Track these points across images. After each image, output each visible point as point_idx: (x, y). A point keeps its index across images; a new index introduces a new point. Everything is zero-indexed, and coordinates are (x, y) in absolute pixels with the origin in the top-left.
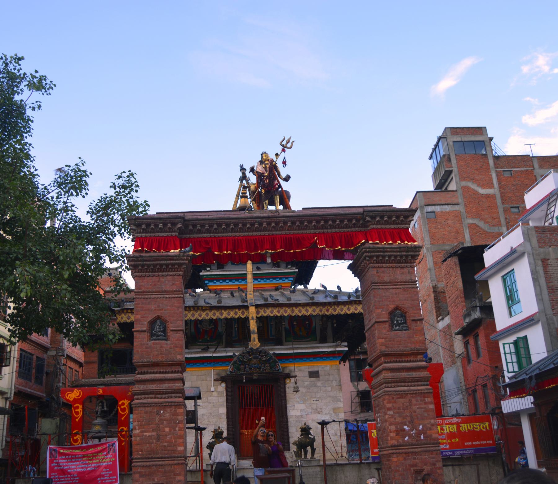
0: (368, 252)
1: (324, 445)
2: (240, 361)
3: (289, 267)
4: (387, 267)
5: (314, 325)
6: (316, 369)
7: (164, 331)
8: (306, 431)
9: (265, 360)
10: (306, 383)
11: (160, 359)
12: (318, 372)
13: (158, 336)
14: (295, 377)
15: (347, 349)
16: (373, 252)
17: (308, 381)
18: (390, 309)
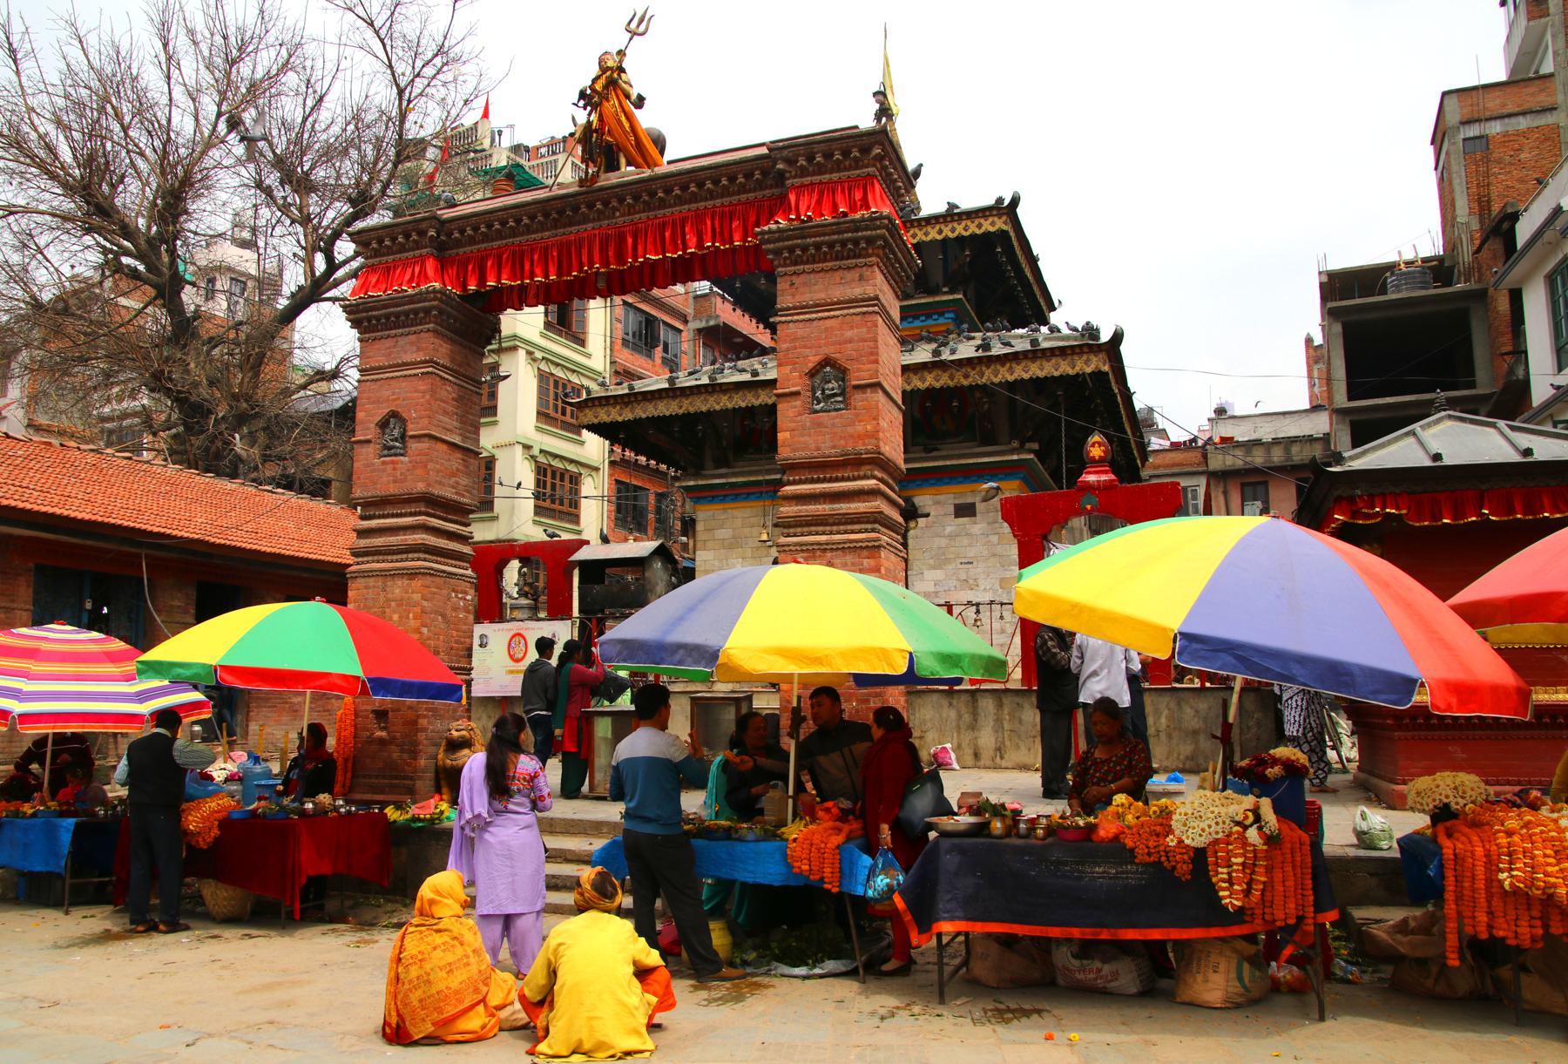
0: (768, 241)
4: (813, 271)
6: (969, 500)
7: (403, 437)
10: (949, 529)
11: (393, 490)
12: (973, 505)
13: (390, 448)
14: (927, 515)
16: (779, 240)
17: (953, 525)
18: (811, 365)
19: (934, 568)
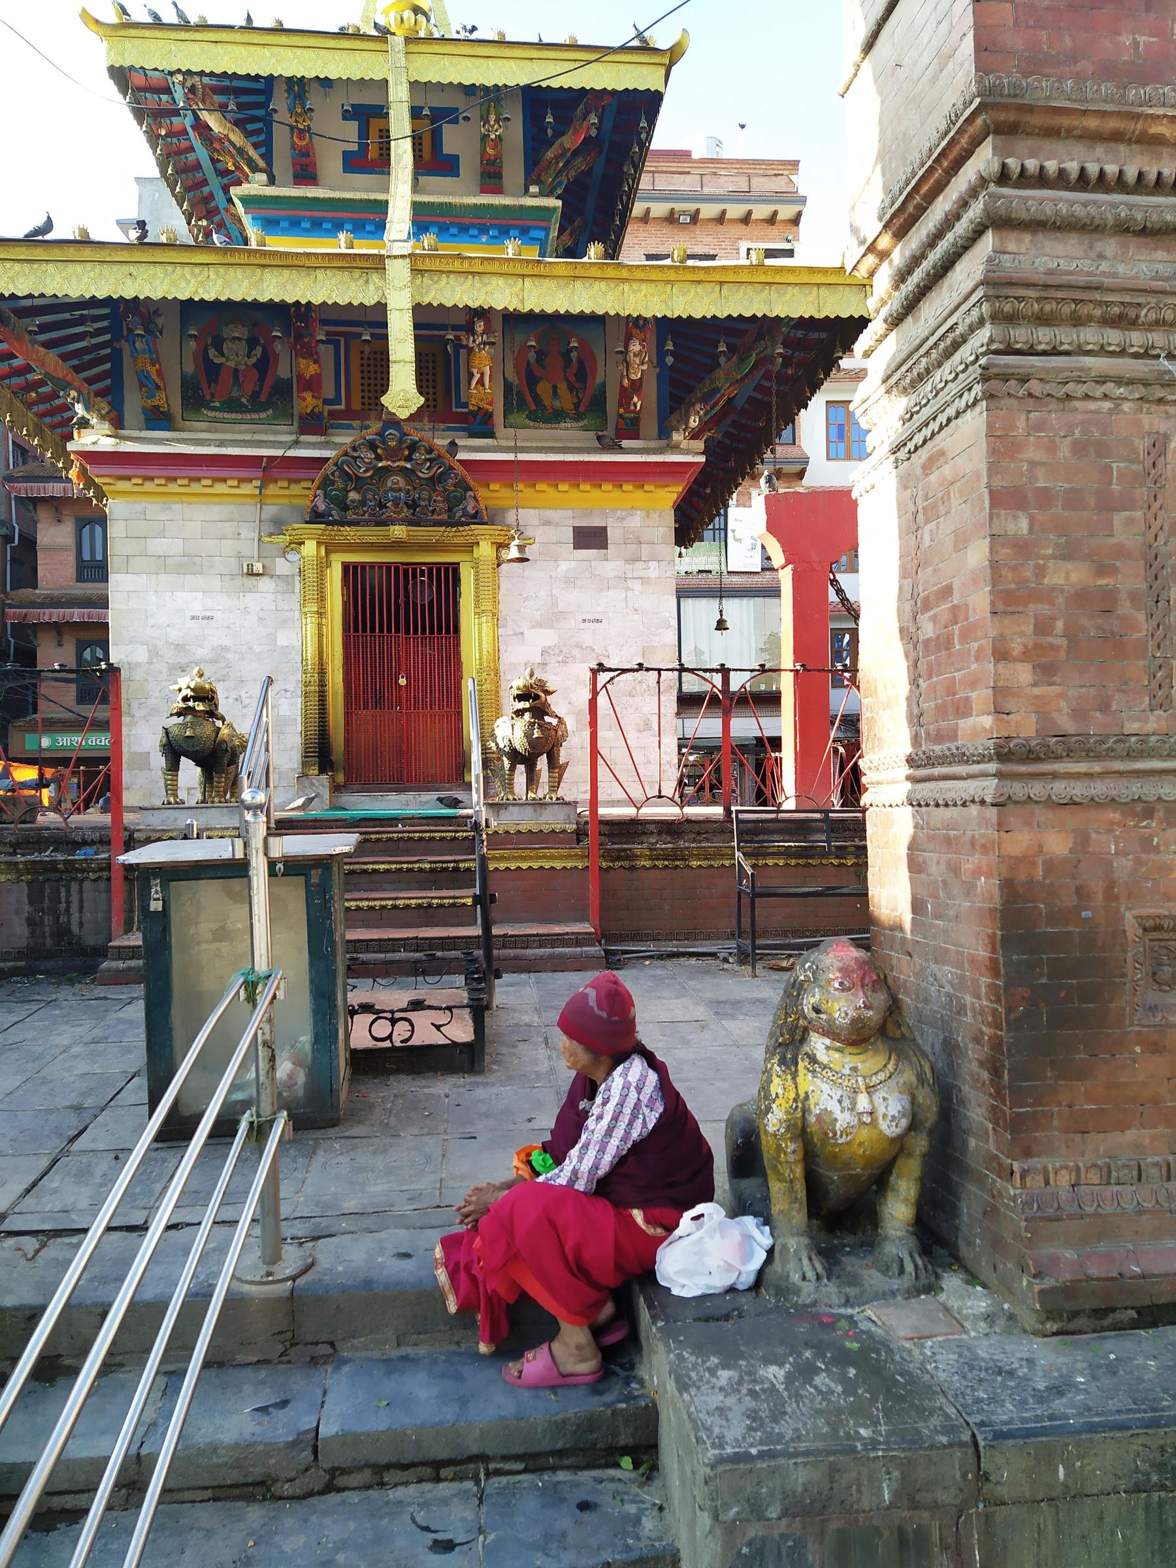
1: (595, 752)
2: (347, 477)
3: (534, 189)
5: (599, 379)
6: (597, 523)
8: (534, 700)
9: (431, 479)
12: (604, 530)
15: (702, 459)
19: (539, 625)
